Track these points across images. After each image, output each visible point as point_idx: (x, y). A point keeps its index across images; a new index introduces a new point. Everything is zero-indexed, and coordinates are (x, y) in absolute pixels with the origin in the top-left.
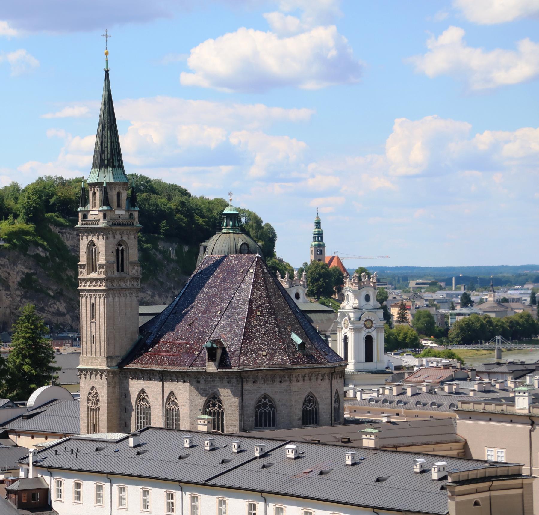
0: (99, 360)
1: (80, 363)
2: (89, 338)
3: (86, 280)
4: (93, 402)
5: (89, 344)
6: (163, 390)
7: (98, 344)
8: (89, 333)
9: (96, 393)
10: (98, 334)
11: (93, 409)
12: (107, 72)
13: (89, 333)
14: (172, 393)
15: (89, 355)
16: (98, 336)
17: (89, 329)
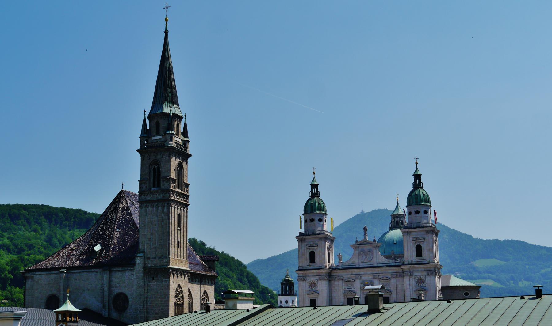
0: (184, 262)
1: (170, 264)
2: (176, 243)
3: (174, 192)
4: (179, 297)
5: (176, 248)
6: (201, 289)
7: (182, 249)
8: (176, 238)
9: (182, 291)
10: (182, 240)
11: (179, 304)
12: (166, 33)
13: (176, 238)
14: (205, 292)
15: (176, 258)
16: (182, 242)
17: (176, 235)
